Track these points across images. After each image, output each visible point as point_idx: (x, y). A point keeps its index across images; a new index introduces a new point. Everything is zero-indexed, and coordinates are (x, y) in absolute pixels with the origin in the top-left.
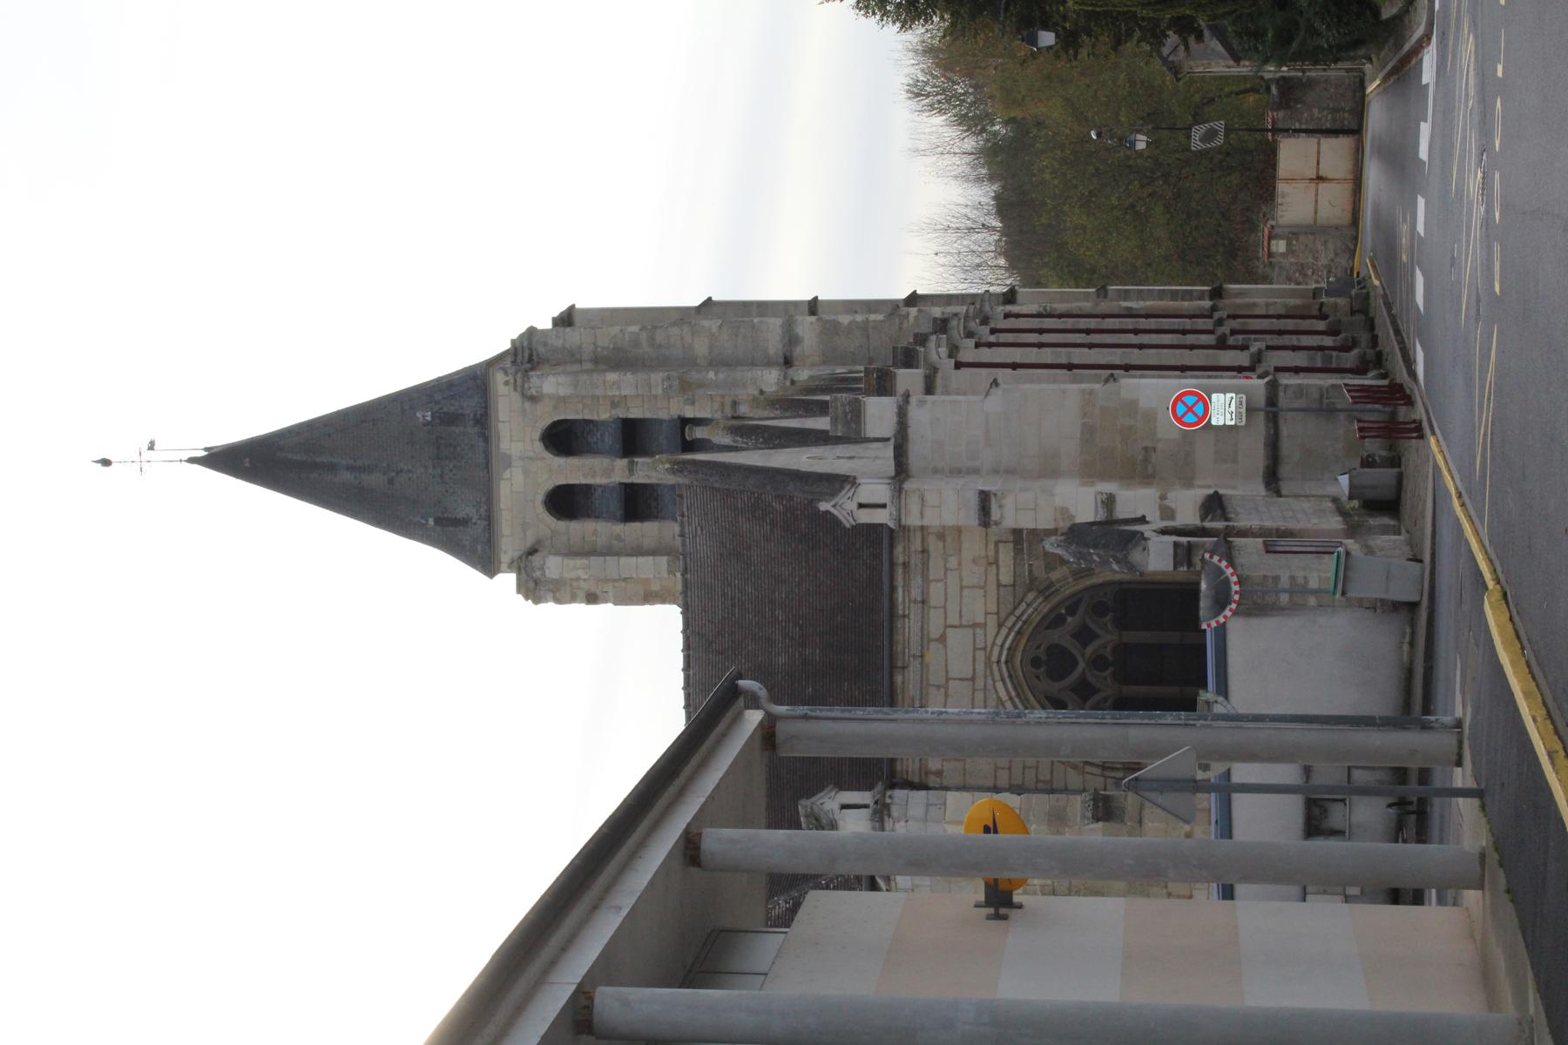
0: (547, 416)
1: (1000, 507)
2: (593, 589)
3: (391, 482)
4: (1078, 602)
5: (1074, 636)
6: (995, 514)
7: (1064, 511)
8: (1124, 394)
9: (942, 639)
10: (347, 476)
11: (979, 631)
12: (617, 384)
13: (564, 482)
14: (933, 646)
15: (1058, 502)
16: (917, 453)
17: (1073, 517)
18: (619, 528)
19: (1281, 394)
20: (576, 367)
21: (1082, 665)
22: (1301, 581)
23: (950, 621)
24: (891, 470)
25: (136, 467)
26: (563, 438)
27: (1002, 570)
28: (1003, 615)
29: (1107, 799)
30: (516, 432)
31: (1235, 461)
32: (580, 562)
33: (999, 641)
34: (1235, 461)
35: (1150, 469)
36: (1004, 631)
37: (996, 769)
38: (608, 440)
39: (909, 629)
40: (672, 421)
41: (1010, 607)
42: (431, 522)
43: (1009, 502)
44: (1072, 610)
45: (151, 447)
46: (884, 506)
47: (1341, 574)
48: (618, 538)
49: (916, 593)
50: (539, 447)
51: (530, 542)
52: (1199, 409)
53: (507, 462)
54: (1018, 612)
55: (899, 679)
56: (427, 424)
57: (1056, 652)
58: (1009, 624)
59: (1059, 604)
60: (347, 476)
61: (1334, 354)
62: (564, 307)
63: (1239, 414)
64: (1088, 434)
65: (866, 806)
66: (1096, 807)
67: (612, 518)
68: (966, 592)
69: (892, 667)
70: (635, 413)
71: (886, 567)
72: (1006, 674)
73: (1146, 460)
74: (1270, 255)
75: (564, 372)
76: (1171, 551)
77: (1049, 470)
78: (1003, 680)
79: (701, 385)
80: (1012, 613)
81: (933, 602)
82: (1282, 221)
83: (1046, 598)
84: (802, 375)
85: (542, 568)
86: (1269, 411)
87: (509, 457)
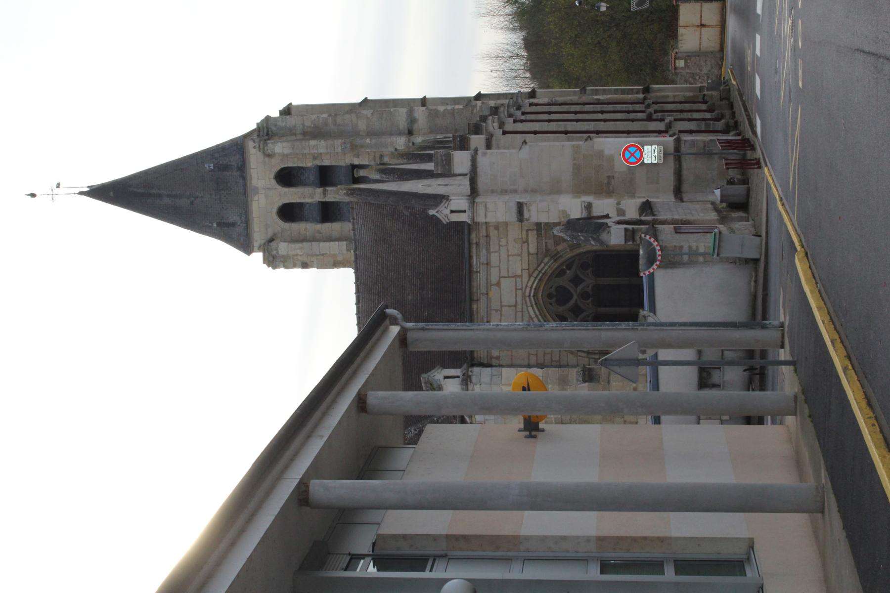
0: (277, 165)
1: (529, 211)
2: (305, 259)
3: (192, 203)
4: (573, 262)
6: (526, 215)
7: (564, 212)
8: (596, 148)
9: (498, 284)
10: (167, 201)
11: (518, 280)
12: (316, 146)
13: (287, 201)
14: (493, 288)
15: (561, 208)
16: (483, 181)
17: (569, 215)
18: (319, 226)
19: (683, 145)
20: (293, 138)
21: (575, 297)
22: (694, 248)
23: (502, 274)
25: (50, 197)
26: (286, 177)
27: (531, 246)
28: (531, 270)
29: (590, 370)
30: (260, 174)
31: (658, 183)
32: (298, 245)
34: (658, 183)
36: (532, 279)
37: (529, 355)
38: (312, 178)
39: (480, 279)
40: (347, 167)
41: (535, 266)
42: (215, 225)
43: (533, 208)
44: (569, 267)
45: (58, 186)
46: (465, 211)
48: (319, 232)
49: (483, 259)
50: (274, 182)
51: (270, 234)
52: (638, 155)
53: (256, 190)
54: (539, 269)
55: (475, 307)
56: (212, 170)
58: (535, 275)
59: (562, 264)
60: (167, 201)
62: (285, 104)
63: (659, 157)
64: (577, 169)
65: (458, 377)
66: (584, 375)
67: (315, 221)
68: (511, 258)
69: (471, 300)
70: (326, 163)
72: (533, 303)
73: (609, 183)
74: (675, 68)
75: (287, 141)
77: (555, 189)
78: (532, 306)
79: (362, 147)
80: (536, 269)
81: (492, 264)
82: (682, 49)
83: (555, 261)
84: (418, 139)
85: (277, 249)
86: (676, 155)
87: (257, 188)
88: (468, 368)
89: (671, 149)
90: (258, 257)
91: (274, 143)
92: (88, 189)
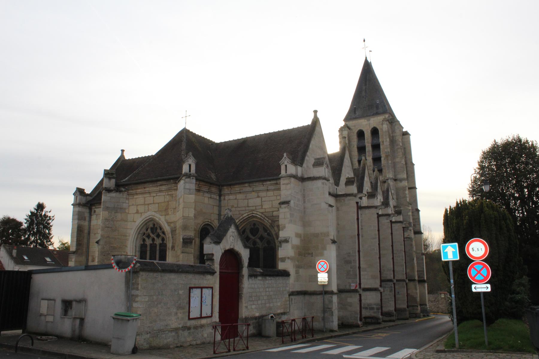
6: (283, 206)
7: (284, 227)
9: (258, 197)
11: (260, 207)
12: (386, 141)
14: (256, 194)
15: (287, 225)
16: (309, 184)
17: (282, 230)
18: (356, 146)
19: (330, 296)
20: (391, 132)
21: (253, 238)
22: (137, 299)
24: (306, 176)
26: (375, 132)
27: (277, 212)
28: (265, 214)
29: (191, 242)
30: (375, 121)
33: (258, 213)
36: (261, 214)
38: (375, 142)
39: (260, 187)
43: (286, 210)
44: (268, 234)
46: (286, 172)
47: (119, 317)
49: (270, 187)
50: (372, 127)
51: (351, 128)
52: (323, 269)
53: (369, 120)
55: (247, 185)
57: (258, 230)
58: (263, 216)
60: (364, 88)
61: (380, 311)
62: (410, 133)
63: (321, 282)
64: (316, 235)
65: (190, 171)
66: (187, 239)
68: (271, 202)
69: (249, 183)
70: (381, 147)
71: (275, 178)
73: (309, 254)
76: (210, 253)
77: (305, 224)
79: (387, 160)
84: (391, 183)
86: (324, 291)
88: (196, 177)
90: (343, 124)
92: (369, 61)
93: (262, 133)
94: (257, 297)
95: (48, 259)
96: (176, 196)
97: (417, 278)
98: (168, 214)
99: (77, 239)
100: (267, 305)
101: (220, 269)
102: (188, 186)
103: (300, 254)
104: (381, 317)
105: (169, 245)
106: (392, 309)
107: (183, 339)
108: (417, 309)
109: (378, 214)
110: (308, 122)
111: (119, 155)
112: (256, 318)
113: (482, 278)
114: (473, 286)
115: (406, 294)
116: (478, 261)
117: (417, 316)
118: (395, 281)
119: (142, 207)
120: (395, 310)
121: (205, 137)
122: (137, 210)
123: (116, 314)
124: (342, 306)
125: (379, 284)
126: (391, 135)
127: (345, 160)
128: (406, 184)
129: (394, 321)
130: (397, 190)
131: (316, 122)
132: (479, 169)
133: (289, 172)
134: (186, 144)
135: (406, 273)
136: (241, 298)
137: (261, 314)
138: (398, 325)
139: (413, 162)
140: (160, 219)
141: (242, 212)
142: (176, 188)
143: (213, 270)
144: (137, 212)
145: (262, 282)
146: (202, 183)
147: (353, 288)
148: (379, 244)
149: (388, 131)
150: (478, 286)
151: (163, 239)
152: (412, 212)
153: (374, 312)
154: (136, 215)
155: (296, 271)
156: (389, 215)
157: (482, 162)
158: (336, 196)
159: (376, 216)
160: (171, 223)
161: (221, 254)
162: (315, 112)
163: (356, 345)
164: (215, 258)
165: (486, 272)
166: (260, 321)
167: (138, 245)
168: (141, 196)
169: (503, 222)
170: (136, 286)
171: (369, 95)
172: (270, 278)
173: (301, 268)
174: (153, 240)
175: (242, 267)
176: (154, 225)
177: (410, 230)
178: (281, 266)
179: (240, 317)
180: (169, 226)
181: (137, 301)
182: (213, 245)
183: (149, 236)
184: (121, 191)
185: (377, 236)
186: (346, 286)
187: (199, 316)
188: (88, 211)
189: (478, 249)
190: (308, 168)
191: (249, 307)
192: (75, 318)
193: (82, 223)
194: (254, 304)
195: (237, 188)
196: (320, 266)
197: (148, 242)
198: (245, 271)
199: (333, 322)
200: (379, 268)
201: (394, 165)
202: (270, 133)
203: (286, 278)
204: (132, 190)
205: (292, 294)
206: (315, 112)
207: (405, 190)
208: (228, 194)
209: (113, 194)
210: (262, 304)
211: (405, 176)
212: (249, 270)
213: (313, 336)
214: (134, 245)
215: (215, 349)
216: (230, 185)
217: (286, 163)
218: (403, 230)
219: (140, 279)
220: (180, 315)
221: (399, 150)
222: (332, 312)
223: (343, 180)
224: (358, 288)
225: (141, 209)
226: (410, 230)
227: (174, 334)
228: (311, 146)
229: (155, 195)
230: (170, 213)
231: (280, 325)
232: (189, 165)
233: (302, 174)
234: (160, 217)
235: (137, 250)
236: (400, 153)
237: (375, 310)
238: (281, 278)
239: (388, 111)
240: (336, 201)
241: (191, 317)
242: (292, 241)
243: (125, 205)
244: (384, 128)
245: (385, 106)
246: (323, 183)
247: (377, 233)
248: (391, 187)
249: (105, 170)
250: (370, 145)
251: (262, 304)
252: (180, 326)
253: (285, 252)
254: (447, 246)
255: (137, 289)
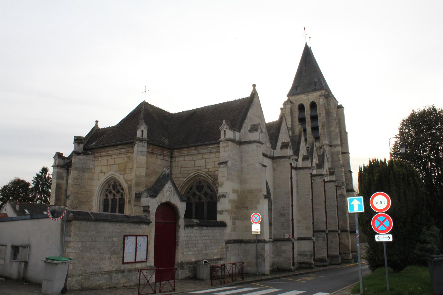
1: (223, 167)
5: (206, 191)
6: (222, 166)
7: (222, 184)
9: (203, 158)
12: (323, 113)
14: (201, 156)
15: (225, 182)
16: (245, 147)
17: (221, 186)
18: (297, 118)
19: (262, 244)
20: (326, 105)
21: (199, 194)
22: (70, 245)
24: (243, 140)
26: (313, 105)
28: (208, 173)
30: (313, 96)
32: (289, 111)
33: (203, 172)
35: (243, 209)
36: (205, 173)
37: (176, 174)
39: (204, 150)
41: (210, 174)
43: (225, 169)
44: (211, 191)
46: (225, 137)
47: (49, 261)
50: (311, 101)
51: (294, 102)
53: (308, 96)
55: (193, 148)
57: (202, 186)
58: (207, 175)
60: (304, 68)
61: (313, 257)
63: (255, 232)
64: (251, 191)
66: (138, 194)
67: (299, 116)
68: (213, 163)
69: (195, 146)
70: (319, 118)
73: (245, 207)
75: (324, 103)
76: (147, 205)
77: (242, 182)
79: (324, 129)
80: (209, 175)
84: (327, 148)
86: (258, 240)
88: (147, 141)
89: (261, 238)
90: (286, 99)
91: (323, 99)
93: (210, 105)
94: (192, 243)
95: (27, 211)
96: (133, 158)
97: (349, 229)
98: (126, 174)
99: (56, 195)
100: (204, 252)
101: (156, 219)
102: (140, 149)
103: (237, 207)
104: (313, 262)
105: (127, 200)
106: (325, 255)
107: (116, 281)
108: (349, 256)
109: (311, 174)
110: (247, 94)
111: (94, 125)
112: (191, 263)
113: (385, 229)
114: (376, 236)
115: (338, 243)
116: (381, 213)
117: (348, 262)
118: (327, 232)
119: (104, 168)
120: (328, 256)
121: (163, 109)
122: (101, 170)
123: (47, 259)
124: (277, 253)
125: (312, 234)
126: (327, 108)
127: (282, 127)
128: (340, 149)
129: (326, 266)
130: (332, 154)
131: (254, 94)
132: (399, 135)
133: (227, 137)
134: (145, 114)
135: (338, 225)
136: (178, 246)
137: (197, 260)
138: (329, 269)
139: (347, 131)
140: (119, 177)
141: (189, 172)
142: (132, 151)
143: (149, 220)
144: (101, 172)
145: (198, 231)
146: (155, 147)
147: (287, 237)
148: (312, 200)
149: (324, 105)
150: (380, 236)
151: (122, 195)
152: (345, 173)
153: (308, 258)
154: (100, 174)
155: (233, 222)
156: (322, 175)
157: (402, 129)
158: (273, 158)
159: (310, 176)
160: (128, 180)
161: (157, 207)
162: (254, 86)
163: (277, 288)
164: (150, 209)
165: (388, 223)
166: (194, 266)
167: (102, 200)
168: (104, 158)
169: (411, 179)
170: (69, 233)
171: (308, 74)
172: (206, 228)
173: (238, 219)
174: (114, 195)
175: (179, 218)
176: (115, 183)
177: (343, 189)
178: (220, 218)
179: (176, 262)
180: (126, 183)
181: (70, 247)
182: (149, 199)
183: (110, 192)
184: (88, 154)
185: (311, 193)
186: (280, 236)
187: (133, 261)
188: (65, 171)
189: (381, 202)
190: (245, 134)
191: (185, 253)
192: (21, 262)
193: (60, 181)
194: (190, 251)
195: (185, 151)
196: (254, 218)
197: (110, 197)
198: (182, 222)
199: (265, 267)
200: (312, 220)
201: (330, 133)
202: (216, 105)
203: (223, 228)
204: (98, 153)
205: (228, 242)
206: (254, 86)
207: (339, 154)
208: (178, 156)
209: (82, 157)
210: (198, 251)
211: (339, 143)
212: (185, 221)
213: (243, 280)
214: (99, 199)
215: (140, 290)
216: (180, 149)
217: (225, 129)
218: (336, 188)
219: (72, 227)
220: (113, 260)
221: (334, 121)
222: (264, 258)
223: (279, 144)
224: (291, 237)
225: (104, 169)
226: (343, 189)
227: (106, 276)
228: (248, 115)
229: (116, 157)
230: (127, 172)
231: (213, 269)
232: (142, 131)
233: (240, 139)
234: (120, 176)
235: (101, 203)
236: (334, 123)
237: (309, 257)
238: (217, 228)
239: (325, 87)
240: (273, 162)
241: (125, 261)
242: (229, 196)
243: (91, 166)
244: (321, 102)
245: (322, 83)
246: (257, 146)
247: (310, 190)
248: (327, 152)
249: (75, 137)
250: (309, 116)
251: (198, 251)
252: (114, 269)
253: (223, 205)
254: (353, 199)
255: (70, 236)
